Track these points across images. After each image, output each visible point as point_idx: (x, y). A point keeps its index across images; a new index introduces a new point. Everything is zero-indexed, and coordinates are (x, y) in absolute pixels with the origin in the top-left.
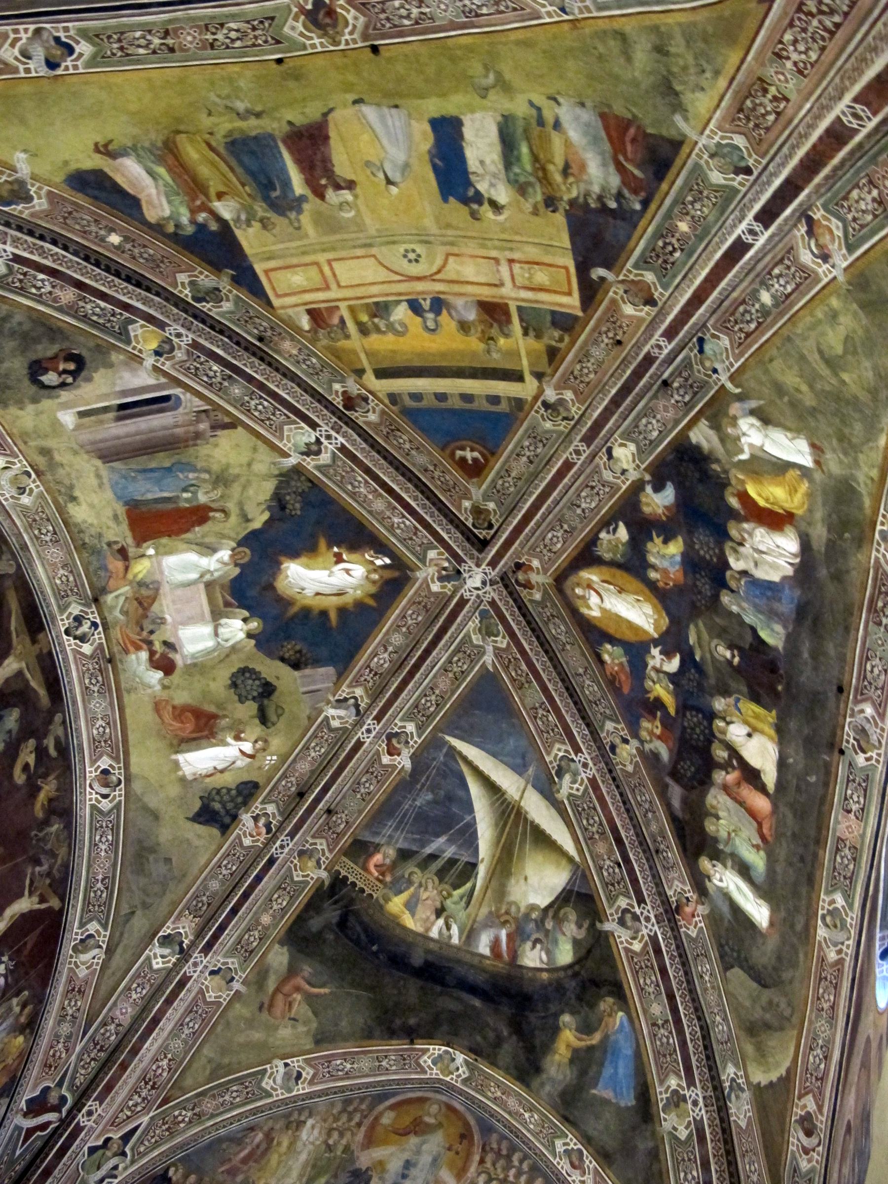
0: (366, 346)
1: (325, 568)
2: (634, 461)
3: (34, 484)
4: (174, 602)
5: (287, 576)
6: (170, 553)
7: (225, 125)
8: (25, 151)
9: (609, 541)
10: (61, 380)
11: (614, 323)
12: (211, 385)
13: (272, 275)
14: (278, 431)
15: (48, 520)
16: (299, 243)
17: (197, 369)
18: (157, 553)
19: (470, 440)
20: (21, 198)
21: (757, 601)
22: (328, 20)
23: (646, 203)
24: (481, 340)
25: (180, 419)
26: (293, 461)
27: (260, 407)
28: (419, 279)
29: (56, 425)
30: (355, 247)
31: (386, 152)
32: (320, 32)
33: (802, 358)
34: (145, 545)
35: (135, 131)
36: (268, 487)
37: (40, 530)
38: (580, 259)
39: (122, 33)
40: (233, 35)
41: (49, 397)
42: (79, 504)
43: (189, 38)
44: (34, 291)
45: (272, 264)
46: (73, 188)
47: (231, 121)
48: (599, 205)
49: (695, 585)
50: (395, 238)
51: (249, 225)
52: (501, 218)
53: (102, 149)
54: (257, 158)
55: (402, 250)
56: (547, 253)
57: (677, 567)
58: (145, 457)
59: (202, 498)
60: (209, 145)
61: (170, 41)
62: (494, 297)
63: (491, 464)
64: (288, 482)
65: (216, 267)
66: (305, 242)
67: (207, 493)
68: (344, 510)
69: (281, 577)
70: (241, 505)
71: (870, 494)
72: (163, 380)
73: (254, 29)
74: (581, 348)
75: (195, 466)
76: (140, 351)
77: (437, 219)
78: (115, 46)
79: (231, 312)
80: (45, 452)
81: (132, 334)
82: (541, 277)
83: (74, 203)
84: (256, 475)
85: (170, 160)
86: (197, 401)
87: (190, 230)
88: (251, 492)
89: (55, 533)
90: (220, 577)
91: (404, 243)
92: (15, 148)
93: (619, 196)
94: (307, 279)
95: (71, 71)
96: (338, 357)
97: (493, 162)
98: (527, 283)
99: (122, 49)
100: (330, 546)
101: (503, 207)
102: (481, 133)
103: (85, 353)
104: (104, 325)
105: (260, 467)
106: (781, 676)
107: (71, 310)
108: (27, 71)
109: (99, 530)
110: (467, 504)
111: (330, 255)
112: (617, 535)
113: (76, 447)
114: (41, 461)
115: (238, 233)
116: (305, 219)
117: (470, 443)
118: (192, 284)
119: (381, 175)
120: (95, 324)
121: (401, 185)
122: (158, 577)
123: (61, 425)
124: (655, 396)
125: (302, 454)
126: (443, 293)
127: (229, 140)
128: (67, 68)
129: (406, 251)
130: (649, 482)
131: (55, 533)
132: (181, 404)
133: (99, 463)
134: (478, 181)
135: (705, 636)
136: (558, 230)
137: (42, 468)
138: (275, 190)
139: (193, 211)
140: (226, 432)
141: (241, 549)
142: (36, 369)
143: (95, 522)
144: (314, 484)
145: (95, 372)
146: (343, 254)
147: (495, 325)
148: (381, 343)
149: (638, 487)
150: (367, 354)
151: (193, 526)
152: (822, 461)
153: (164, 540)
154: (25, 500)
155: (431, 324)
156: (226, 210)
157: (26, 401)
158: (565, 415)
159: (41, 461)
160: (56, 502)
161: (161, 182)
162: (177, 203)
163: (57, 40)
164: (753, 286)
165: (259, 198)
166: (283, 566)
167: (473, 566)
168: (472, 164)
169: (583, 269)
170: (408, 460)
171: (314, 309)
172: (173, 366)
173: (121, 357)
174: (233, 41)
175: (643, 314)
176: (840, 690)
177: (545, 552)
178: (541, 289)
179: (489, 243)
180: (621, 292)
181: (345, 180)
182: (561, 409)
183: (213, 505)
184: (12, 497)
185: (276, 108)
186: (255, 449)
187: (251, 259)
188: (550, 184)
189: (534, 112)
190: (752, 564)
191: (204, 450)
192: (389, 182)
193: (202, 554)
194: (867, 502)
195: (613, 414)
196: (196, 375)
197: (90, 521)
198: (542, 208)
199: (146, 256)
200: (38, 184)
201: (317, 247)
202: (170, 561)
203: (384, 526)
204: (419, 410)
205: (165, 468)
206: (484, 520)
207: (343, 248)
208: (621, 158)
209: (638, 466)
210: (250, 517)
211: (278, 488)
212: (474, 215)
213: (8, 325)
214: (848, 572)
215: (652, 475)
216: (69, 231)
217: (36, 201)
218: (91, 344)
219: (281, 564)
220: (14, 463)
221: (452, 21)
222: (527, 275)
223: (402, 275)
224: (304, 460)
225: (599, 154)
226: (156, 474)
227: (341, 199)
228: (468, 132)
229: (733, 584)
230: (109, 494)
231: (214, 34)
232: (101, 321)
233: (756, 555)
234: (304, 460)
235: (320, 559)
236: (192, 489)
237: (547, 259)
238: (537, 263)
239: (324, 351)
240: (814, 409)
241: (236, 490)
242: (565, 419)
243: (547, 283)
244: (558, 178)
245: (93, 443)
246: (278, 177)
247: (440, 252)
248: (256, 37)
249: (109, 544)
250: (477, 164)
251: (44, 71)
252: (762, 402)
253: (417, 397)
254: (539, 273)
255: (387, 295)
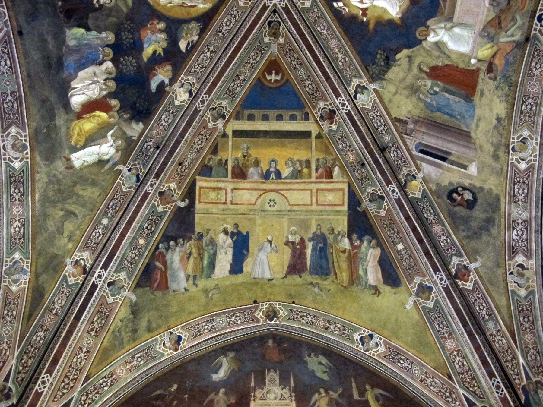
0: (310, 153)
1: (375, 6)
2: (176, 95)
3: (515, 140)
4: (477, 15)
5: (400, 7)
6: (462, 55)
7: (326, 283)
8: (405, 308)
9: (192, 35)
10: (464, 192)
11: (181, 176)
12: (398, 148)
13: (341, 203)
14: (374, 107)
15: (521, 113)
16: (321, 217)
17: (401, 159)
18: (470, 60)
19: (271, 88)
20: (423, 287)
21: (90, 51)
22: (270, 313)
23: (157, 248)
24: (250, 156)
25: (420, 136)
26: (373, 86)
27: (379, 124)
28: (272, 191)
29: (480, 170)
30: (297, 211)
31: (267, 256)
32: (275, 309)
33: (84, 206)
34: (474, 68)
35: (360, 295)
36: (390, 75)
37: (531, 109)
38: (192, 209)
39: (341, 335)
40: (305, 318)
41: (474, 186)
42: (498, 115)
43: (320, 323)
44: (449, 241)
45: (339, 208)
46: (400, 281)
47: (323, 284)
48: (178, 241)
49: (132, 34)
50: (277, 213)
51: (339, 232)
52: (225, 226)
53: (378, 292)
54: (320, 265)
55: (276, 206)
56: (207, 210)
57: (146, 39)
58: (447, 124)
59: (429, 83)
60: (336, 277)
61: (327, 325)
62: (238, 182)
63: (262, 71)
64: (379, 73)
65: (365, 214)
66: (318, 217)
67: (425, 85)
68: (354, 46)
69: (403, 8)
70: (410, 69)
71: (38, 163)
72: (418, 162)
73: (297, 318)
74: (200, 156)
75: (424, 105)
76: (421, 183)
77: (254, 223)
78: (346, 332)
79: (370, 185)
80: (496, 157)
81: (421, 193)
82: (212, 195)
83: (404, 273)
84: (395, 85)
85: (355, 276)
86: (408, 143)
87: (366, 238)
88: (401, 75)
89: (523, 102)
90: (441, 22)
91: (273, 211)
92: (408, 312)
93: (167, 249)
94: (325, 196)
95: (367, 330)
96: (327, 147)
97: (221, 254)
98: (220, 192)
99: (345, 330)
100: (368, 22)
101: (222, 232)
102: (222, 268)
103: (445, 197)
104: (430, 205)
105: (391, 88)
106: (61, 12)
107: (439, 221)
108: (381, 339)
109: (496, 92)
110: (281, 40)
111: (310, 208)
112: (187, 42)
113: (478, 149)
114: (501, 154)
115: (346, 230)
116: (314, 229)
117: (271, 85)
118: (379, 208)
119: (273, 245)
120: (433, 208)
121: (266, 240)
122: (479, 40)
123: (478, 168)
124: (163, 138)
125: (366, 88)
126: (262, 183)
127: (327, 277)
128: (368, 332)
129: (274, 206)
130: (167, 86)
131: (523, 102)
132: (417, 144)
133: (473, 134)
134: (231, 244)
135: (120, 4)
136: (199, 222)
137: (503, 148)
138: (320, 247)
139: (359, 247)
140: (401, 118)
141: (421, 38)
142: (470, 205)
143: (495, 98)
144: (366, 68)
145: (446, 186)
146: (303, 208)
147: (241, 165)
148: (301, 155)
149: (173, 80)
150: (311, 149)
151: (441, 67)
152: (66, 162)
153: (462, 65)
154: (526, 133)
155: (273, 164)
156: (345, 243)
157: (486, 191)
158: (214, 111)
159: (501, 154)
160: (510, 124)
161: (364, 267)
162: (364, 254)
163: (363, 345)
164: (111, 223)
165: (328, 244)
166: (400, 16)
167: (278, 5)
168: (230, 252)
169: (192, 204)
170: (310, 72)
171: (329, 179)
172: (410, 167)
173: (431, 185)
174: (306, 316)
175: (166, 185)
176: (20, 33)
177: (235, 13)
178: (214, 188)
179: (233, 212)
180: (175, 195)
181: (289, 246)
182: (216, 115)
183: (424, 75)
184: (532, 139)
185: (303, 285)
186: (390, 101)
187: (347, 214)
188: (198, 247)
189: (196, 282)
190: (97, 72)
191: (416, 112)
192: (270, 242)
193: (445, 44)
194: (38, 158)
195: (180, 134)
196: (402, 156)
197: (498, 100)
198: (205, 234)
199: (392, 232)
200: (411, 290)
201: (314, 213)
202: (464, 49)
203: (333, 30)
204: (295, 109)
205: (440, 112)
206: (273, 28)
207: (302, 211)
208: (163, 269)
209: (173, 93)
210: (407, 59)
211: (386, 72)
212: (236, 226)
213: (469, 234)
214: (39, 110)
215: (165, 91)
216: (416, 260)
217: (418, 283)
218: (440, 200)
219: (400, 18)
220: (516, 160)
221: (219, 316)
222: (219, 196)
223: (280, 193)
224: (367, 84)
225: (174, 268)
226: (447, 111)
227: (294, 236)
228: (228, 267)
229: (108, 50)
230: (478, 112)
231: (311, 321)
232: (430, 208)
233: (96, 79)
234: (367, 84)
235: (376, 14)
236: (432, 92)
237: (208, 206)
238: (213, 203)
239: (333, 153)
240: (75, 186)
241: (409, 80)
242: (214, 109)
243: (210, 193)
244: (194, 251)
245: (469, 148)
246: (316, 254)
247: (257, 207)
248: (298, 314)
249: (495, 79)
250: (228, 253)
251: (376, 335)
252: (103, 171)
253: (293, 118)
254: (213, 198)
255: (290, 183)
